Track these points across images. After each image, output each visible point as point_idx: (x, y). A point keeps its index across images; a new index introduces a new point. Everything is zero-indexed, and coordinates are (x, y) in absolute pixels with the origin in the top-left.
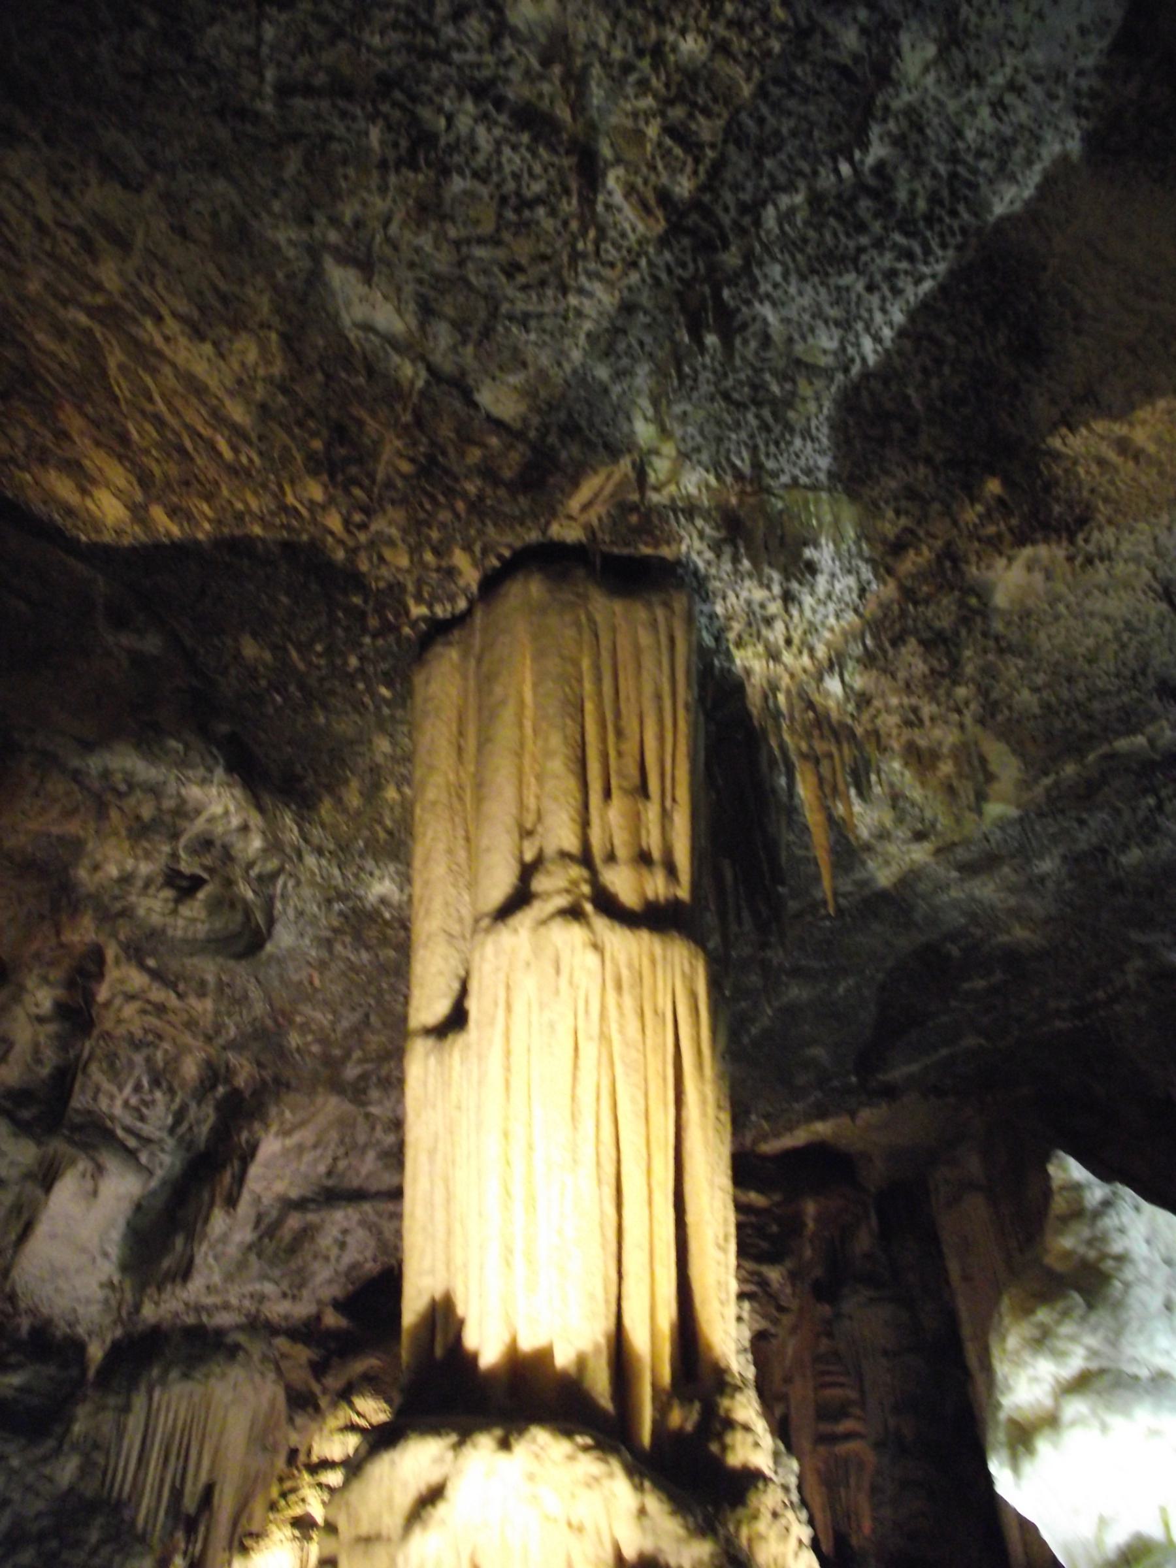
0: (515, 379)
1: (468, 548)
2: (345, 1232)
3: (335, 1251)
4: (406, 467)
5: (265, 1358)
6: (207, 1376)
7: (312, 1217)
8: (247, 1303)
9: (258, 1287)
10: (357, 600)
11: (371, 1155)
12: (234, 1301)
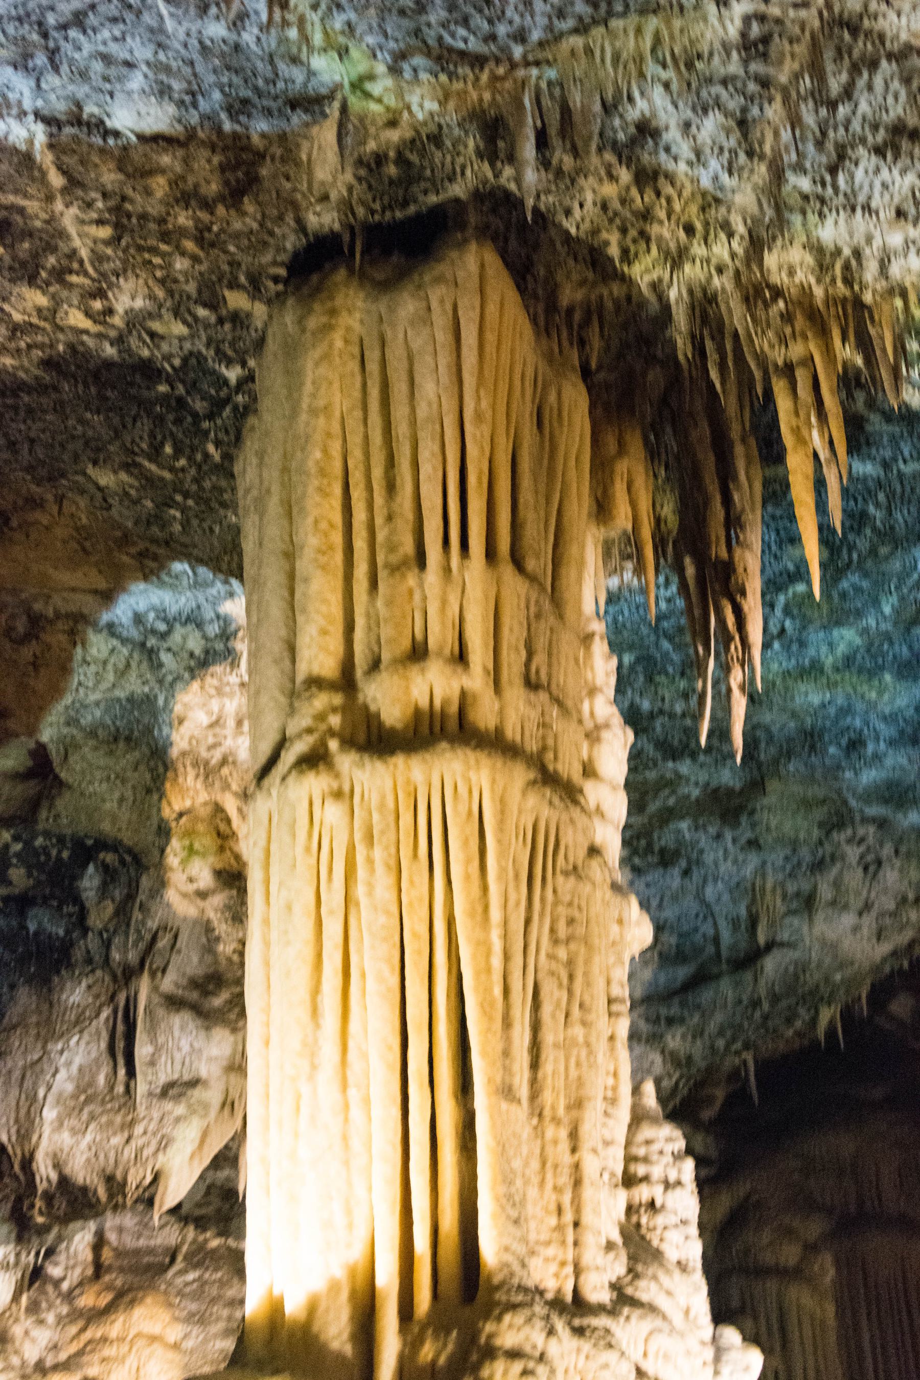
0: (136, 81)
1: (234, 285)
4: (105, 232)
10: (163, 388)
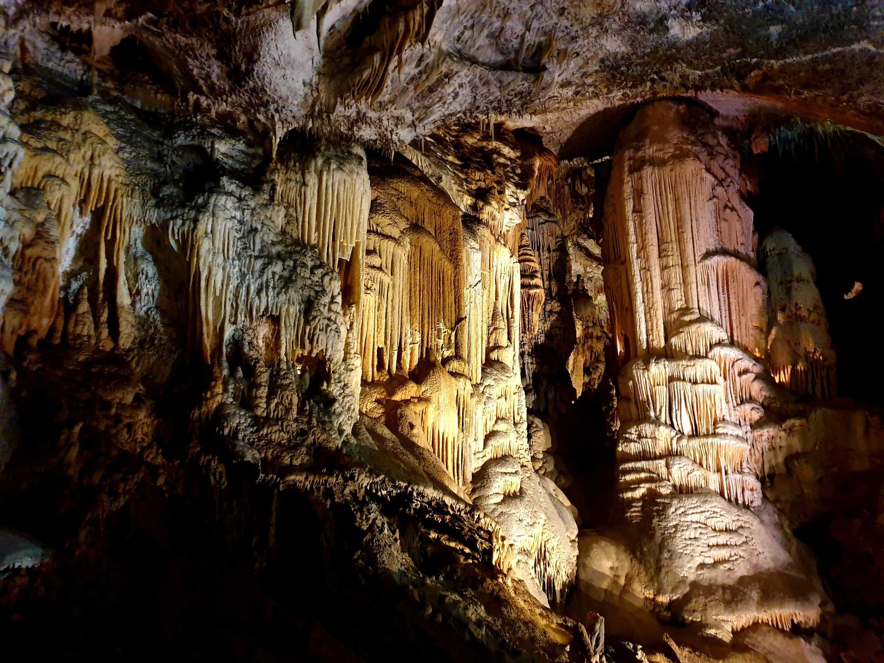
6: (352, 172)
7: (455, 67)
9: (403, 111)
11: (486, 32)
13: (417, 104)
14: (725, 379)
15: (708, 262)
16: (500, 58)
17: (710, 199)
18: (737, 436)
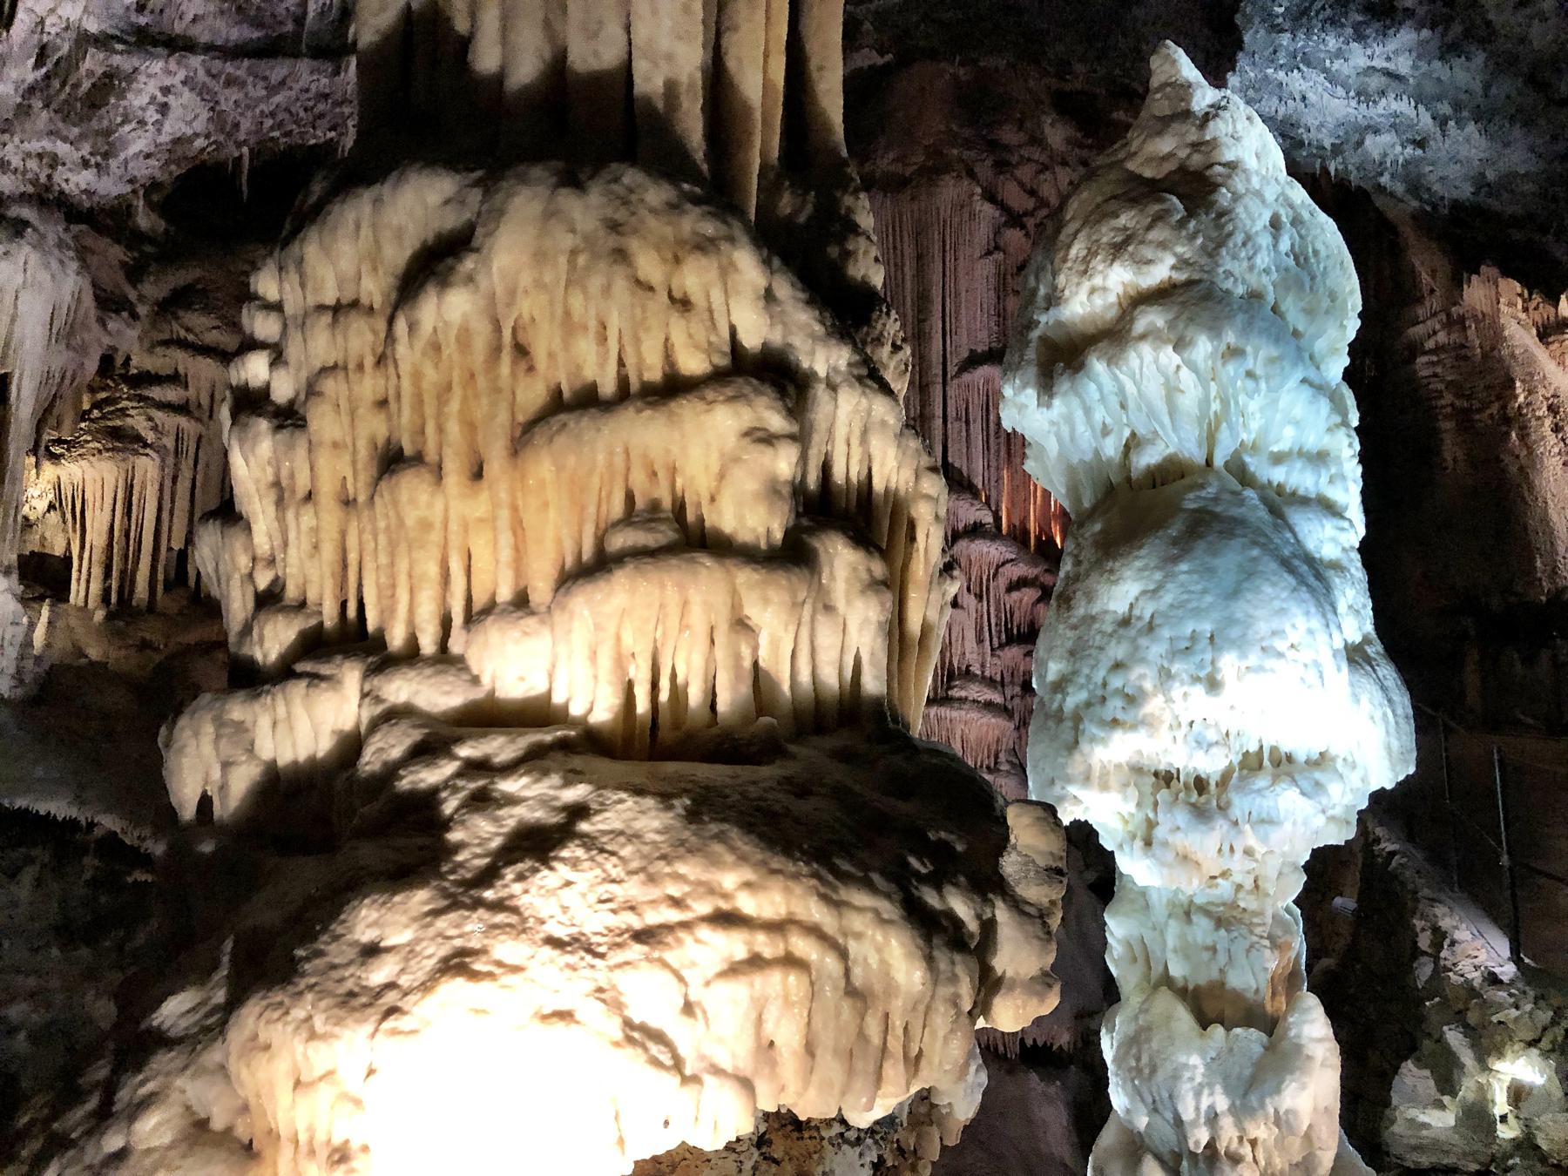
2: (166, 90)
3: (152, 115)
5: (61, 244)
8: (32, 164)
9: (47, 144)
12: (16, 162)
13: (76, 131)
14: (979, 597)
15: (966, 377)
16: (256, 34)
17: (989, 253)
18: (989, 706)
